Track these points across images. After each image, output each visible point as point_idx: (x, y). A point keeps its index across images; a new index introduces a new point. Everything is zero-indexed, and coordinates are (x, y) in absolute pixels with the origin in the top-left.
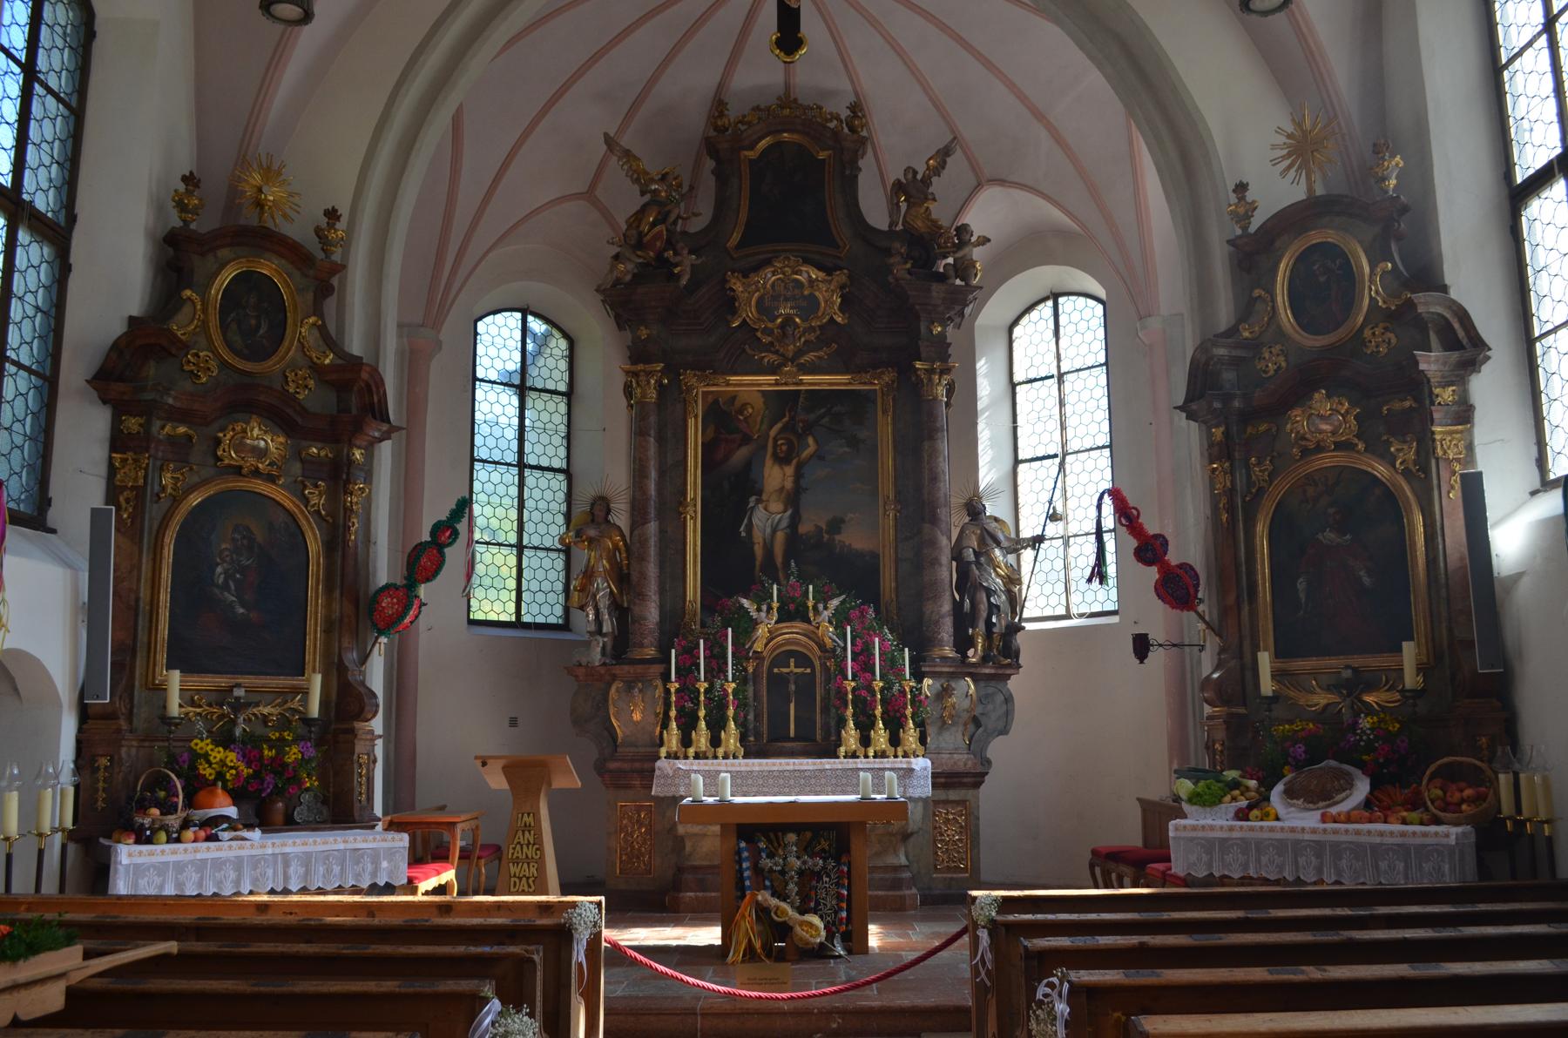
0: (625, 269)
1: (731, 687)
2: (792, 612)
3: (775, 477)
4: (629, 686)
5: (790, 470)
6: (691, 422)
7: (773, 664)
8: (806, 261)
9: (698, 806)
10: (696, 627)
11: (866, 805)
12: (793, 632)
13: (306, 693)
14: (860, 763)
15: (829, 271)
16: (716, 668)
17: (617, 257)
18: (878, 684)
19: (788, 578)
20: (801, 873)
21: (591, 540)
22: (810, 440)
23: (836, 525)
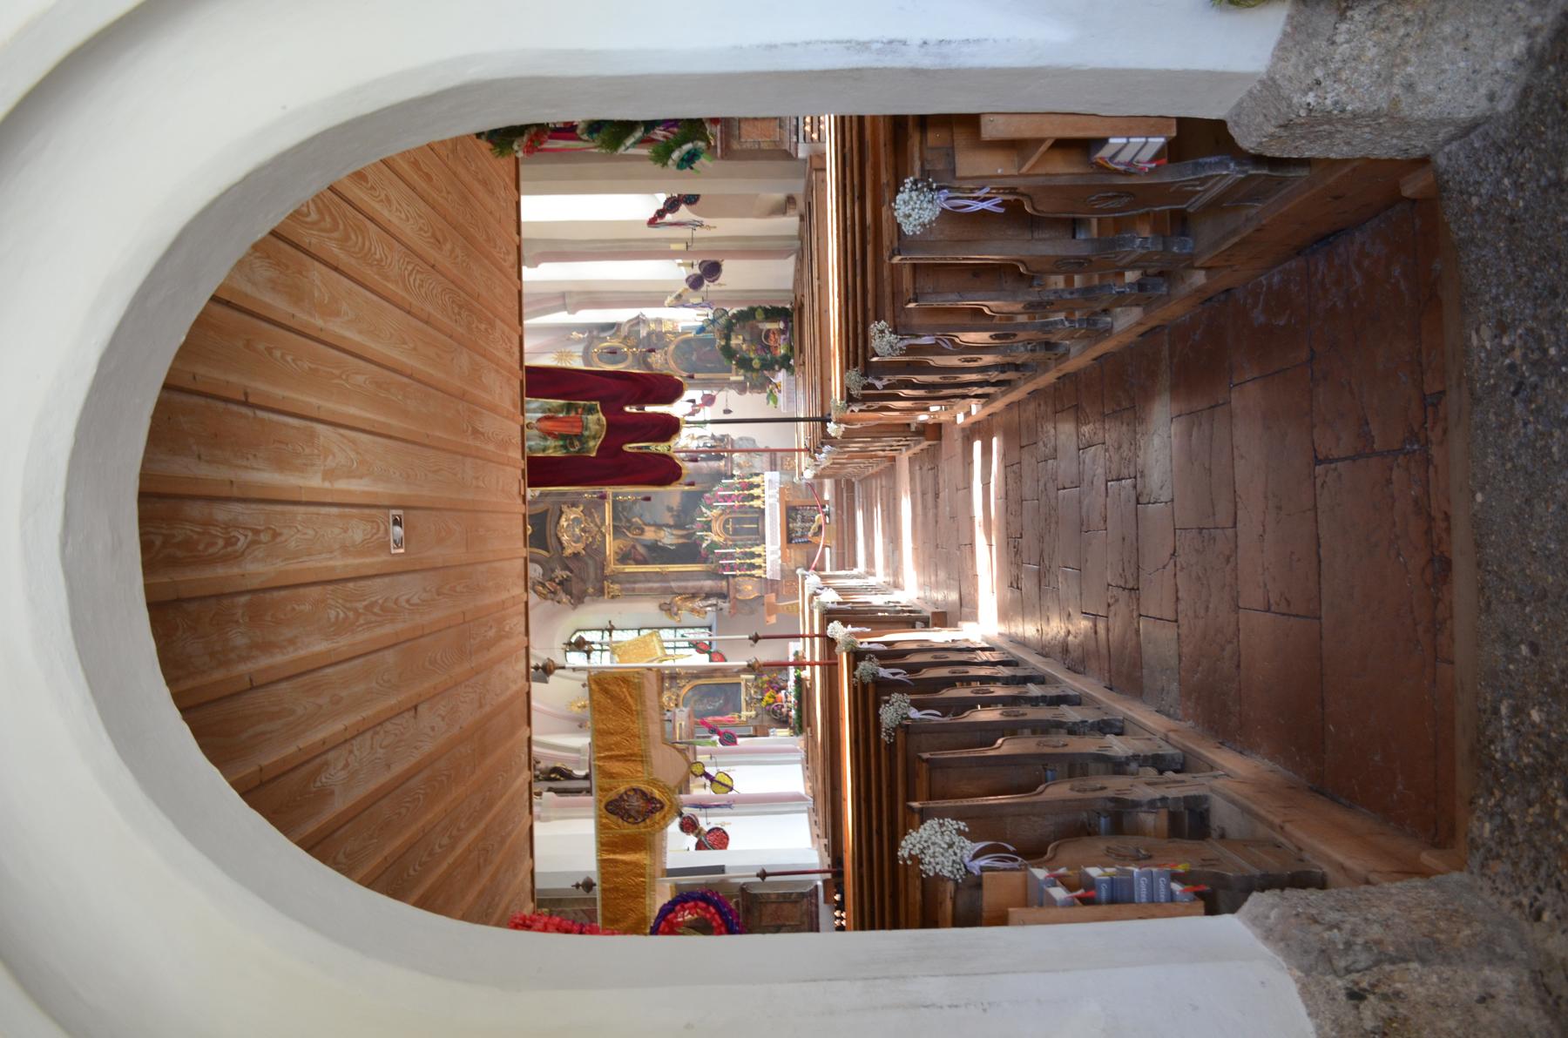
0: (565, 598)
1: (738, 550)
2: (707, 527)
3: (650, 535)
4: (738, 591)
5: (646, 528)
6: (627, 570)
7: (728, 534)
8: (558, 522)
9: (783, 557)
10: (713, 566)
11: (781, 500)
12: (716, 526)
13: (747, 680)
14: (767, 499)
15: (562, 513)
16: (731, 556)
17: (559, 602)
18: (736, 492)
19: (692, 529)
20: (803, 522)
21: (678, 610)
22: (634, 520)
23: (670, 509)
